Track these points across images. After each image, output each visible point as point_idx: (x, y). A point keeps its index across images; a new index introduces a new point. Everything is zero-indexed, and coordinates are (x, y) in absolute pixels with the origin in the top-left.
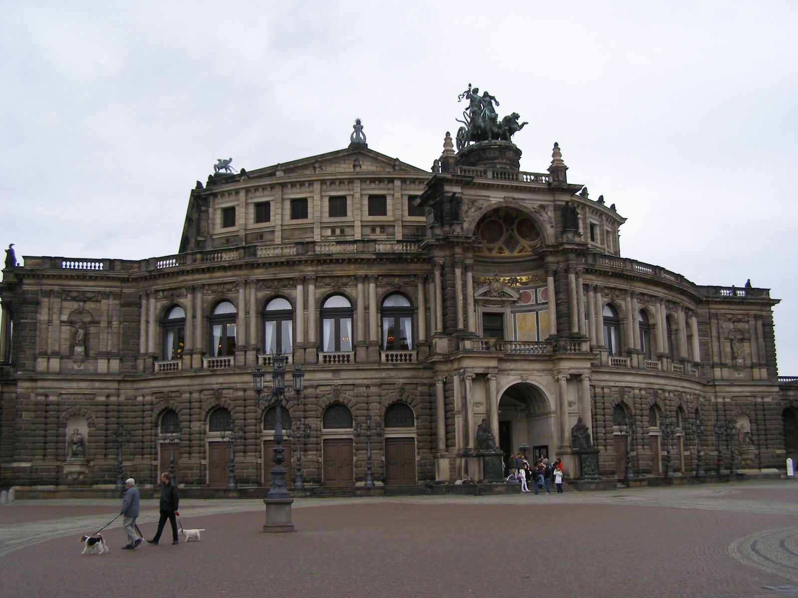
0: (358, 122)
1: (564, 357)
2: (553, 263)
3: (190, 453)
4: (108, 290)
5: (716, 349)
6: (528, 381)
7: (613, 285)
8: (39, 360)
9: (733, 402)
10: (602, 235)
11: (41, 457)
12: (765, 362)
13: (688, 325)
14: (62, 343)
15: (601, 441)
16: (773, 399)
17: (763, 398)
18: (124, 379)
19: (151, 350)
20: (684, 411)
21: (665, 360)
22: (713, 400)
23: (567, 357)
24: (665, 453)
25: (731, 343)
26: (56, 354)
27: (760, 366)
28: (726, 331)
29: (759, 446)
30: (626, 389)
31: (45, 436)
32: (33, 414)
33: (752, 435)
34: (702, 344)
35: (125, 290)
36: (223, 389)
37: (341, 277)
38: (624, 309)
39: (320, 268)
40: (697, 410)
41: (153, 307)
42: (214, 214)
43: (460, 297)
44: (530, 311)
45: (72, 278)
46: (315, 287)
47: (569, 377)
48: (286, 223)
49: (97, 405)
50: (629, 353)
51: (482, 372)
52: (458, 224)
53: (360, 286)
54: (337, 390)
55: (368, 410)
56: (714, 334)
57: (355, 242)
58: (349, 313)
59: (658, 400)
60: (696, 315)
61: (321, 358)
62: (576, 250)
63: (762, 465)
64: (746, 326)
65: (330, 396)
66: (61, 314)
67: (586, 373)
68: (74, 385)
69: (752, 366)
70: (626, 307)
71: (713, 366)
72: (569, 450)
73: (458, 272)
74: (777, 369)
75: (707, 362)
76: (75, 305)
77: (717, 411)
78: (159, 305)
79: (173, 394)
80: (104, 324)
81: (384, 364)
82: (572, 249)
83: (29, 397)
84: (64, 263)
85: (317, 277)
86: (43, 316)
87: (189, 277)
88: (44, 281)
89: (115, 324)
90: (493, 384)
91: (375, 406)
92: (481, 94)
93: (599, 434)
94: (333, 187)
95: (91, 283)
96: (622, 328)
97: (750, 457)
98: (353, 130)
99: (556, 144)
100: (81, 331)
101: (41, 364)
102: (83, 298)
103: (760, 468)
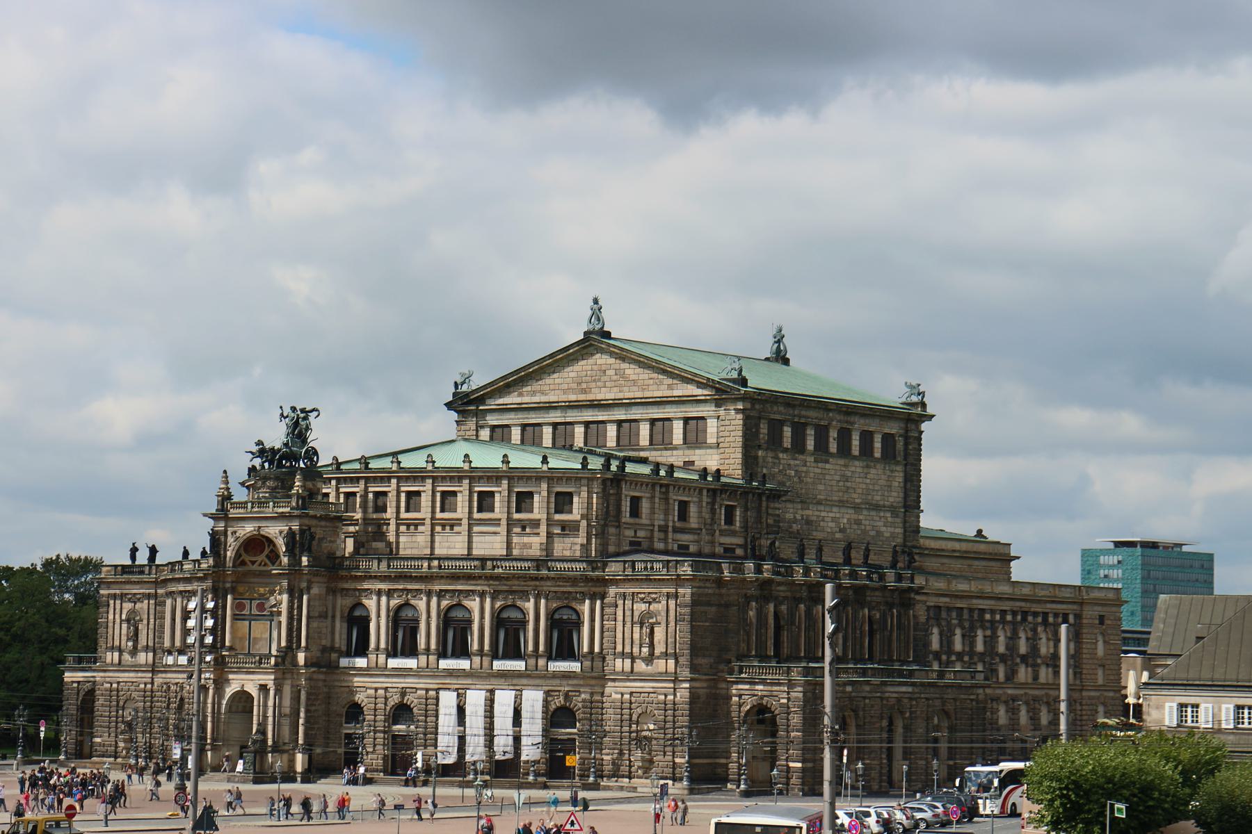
0: (596, 301)
5: (619, 635)
7: (401, 587)
18: (154, 669)
21: (477, 660)
22: (614, 696)
26: (121, 651)
27: (666, 655)
35: (159, 591)
56: (620, 617)
68: (126, 674)
80: (145, 622)
86: (111, 617)
89: (152, 621)
98: (590, 312)
102: (135, 599)
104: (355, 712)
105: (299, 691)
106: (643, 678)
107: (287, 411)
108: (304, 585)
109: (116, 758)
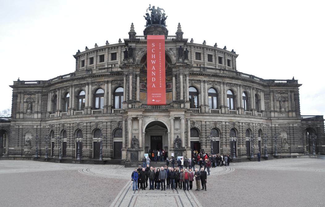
1: (171, 110)
2: (175, 71)
3: (57, 146)
4: (38, 91)
6: (158, 120)
8: (17, 115)
9: (279, 126)
10: (225, 61)
11: (17, 146)
12: (295, 110)
13: (257, 96)
14: (24, 108)
15: (204, 143)
16: (298, 125)
17: (293, 125)
18: (42, 120)
19: (50, 111)
20: (251, 131)
22: (270, 125)
23: (173, 110)
24: (239, 148)
25: (280, 102)
26: (23, 113)
27: (292, 111)
28: (277, 97)
29: (290, 144)
30: (218, 122)
31: (18, 139)
32: (15, 132)
33: (288, 140)
34: (266, 103)
36: (65, 124)
37: (100, 82)
38: (219, 89)
39: (93, 79)
40: (260, 130)
41: (51, 95)
42: (79, 63)
43: (131, 87)
44: (170, 92)
45: (27, 87)
46: (92, 85)
47: (174, 118)
48: (98, 64)
49: (34, 129)
50: (221, 108)
51: (135, 117)
52: (131, 58)
53: (106, 85)
54: (97, 124)
55: (106, 131)
56: (272, 99)
57: (105, 69)
58: (102, 95)
59: (236, 127)
60: (263, 91)
61: (92, 112)
62: (182, 66)
63: (291, 152)
64: (287, 95)
65: (95, 126)
66: (24, 99)
67: (182, 117)
68: (27, 122)
69: (289, 112)
70: (220, 89)
71: (271, 112)
72: (172, 149)
73: (131, 77)
74: (300, 113)
75: (268, 110)
76: (28, 96)
77: (272, 130)
78: (52, 95)
79: (53, 125)
80: (36, 102)
81: (113, 114)
82: (180, 65)
83: (14, 127)
84: (25, 83)
85: (92, 83)
86: (18, 100)
87: (58, 85)
88: (19, 89)
89: (40, 102)
90: (140, 122)
91: (109, 130)
92: (156, 8)
93: (203, 141)
94: (112, 50)
95: (33, 89)
96: (218, 97)
97: (286, 148)
99: (179, 24)
100: (29, 105)
101: (18, 116)
102: (30, 94)
103: (291, 153)
104: (195, 131)
105: (187, 121)
106: (283, 119)
107: (151, 8)
108: (187, 73)
109: (22, 155)
